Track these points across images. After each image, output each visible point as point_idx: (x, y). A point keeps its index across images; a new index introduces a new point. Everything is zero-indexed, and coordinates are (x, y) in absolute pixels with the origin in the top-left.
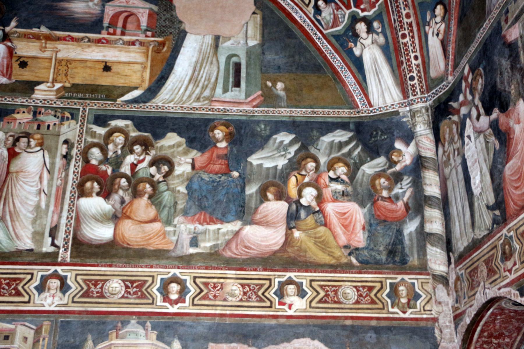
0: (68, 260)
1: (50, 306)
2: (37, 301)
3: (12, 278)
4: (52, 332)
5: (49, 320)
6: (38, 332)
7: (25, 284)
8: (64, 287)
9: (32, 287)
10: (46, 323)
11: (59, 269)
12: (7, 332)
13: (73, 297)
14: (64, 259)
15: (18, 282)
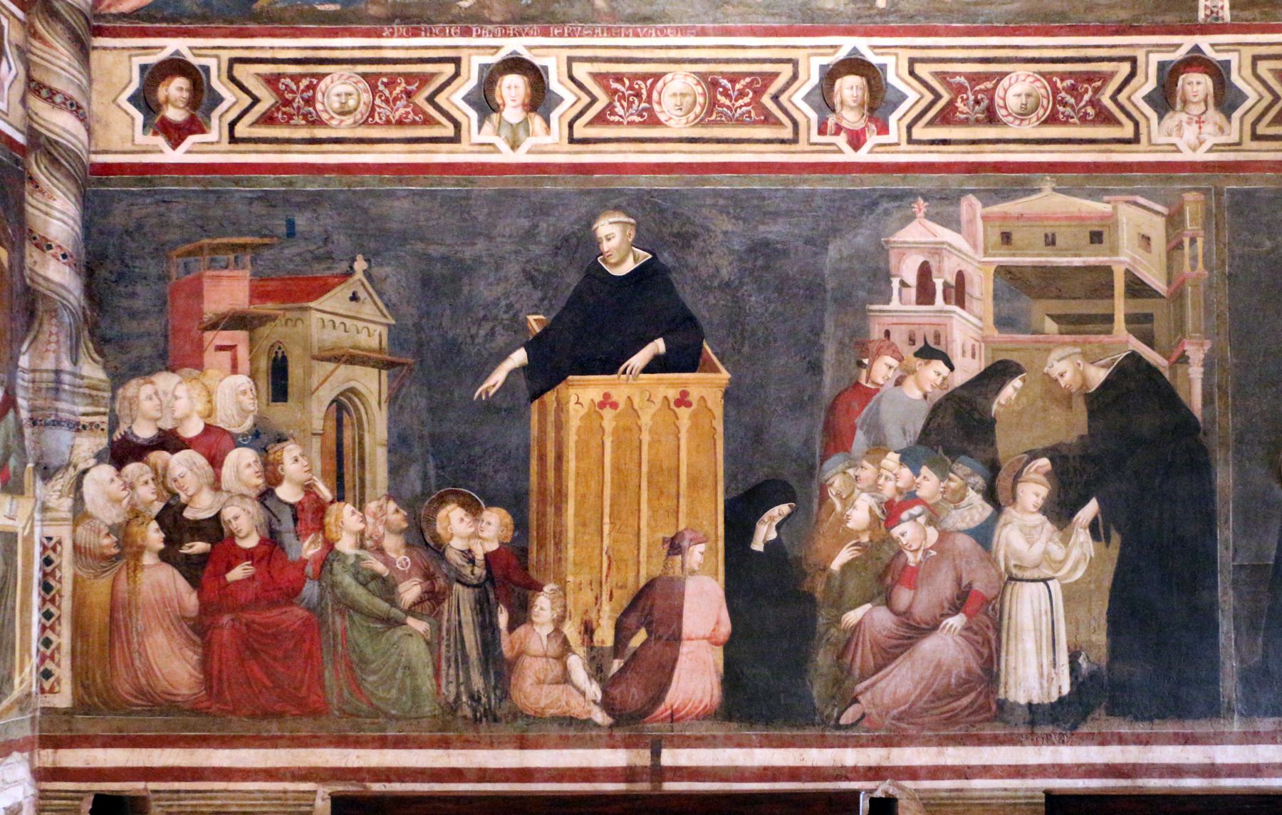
0: (1226, 15)
1: (1194, 150)
2: (1159, 138)
3: (1081, 73)
4: (1211, 219)
5: (1195, 189)
6: (1174, 221)
7: (1119, 90)
8: (1226, 98)
9: (1138, 98)
10: (1189, 197)
11: (1204, 42)
12: (1095, 222)
13: (1254, 125)
14: (1213, 12)
15: (1099, 84)
